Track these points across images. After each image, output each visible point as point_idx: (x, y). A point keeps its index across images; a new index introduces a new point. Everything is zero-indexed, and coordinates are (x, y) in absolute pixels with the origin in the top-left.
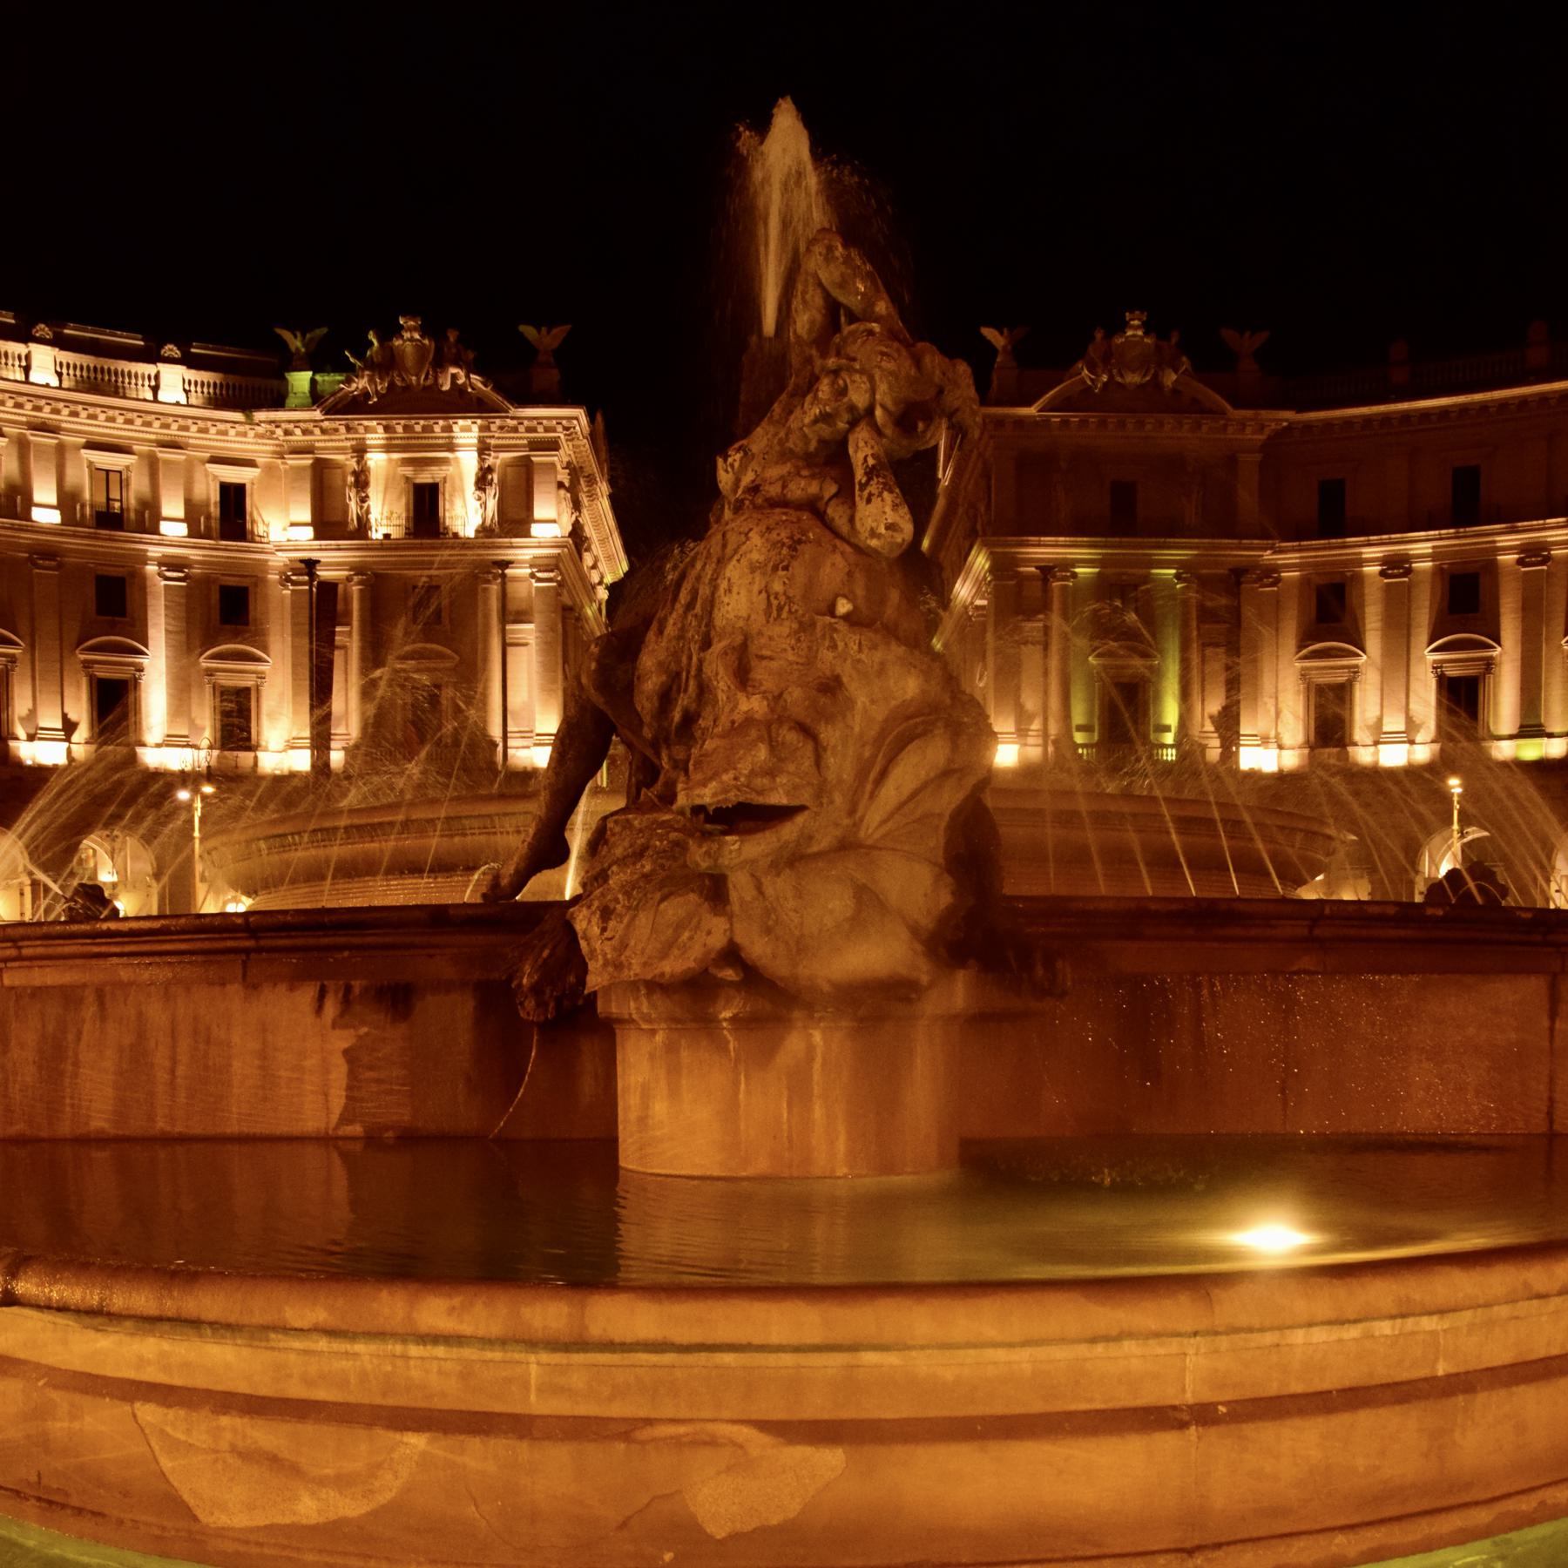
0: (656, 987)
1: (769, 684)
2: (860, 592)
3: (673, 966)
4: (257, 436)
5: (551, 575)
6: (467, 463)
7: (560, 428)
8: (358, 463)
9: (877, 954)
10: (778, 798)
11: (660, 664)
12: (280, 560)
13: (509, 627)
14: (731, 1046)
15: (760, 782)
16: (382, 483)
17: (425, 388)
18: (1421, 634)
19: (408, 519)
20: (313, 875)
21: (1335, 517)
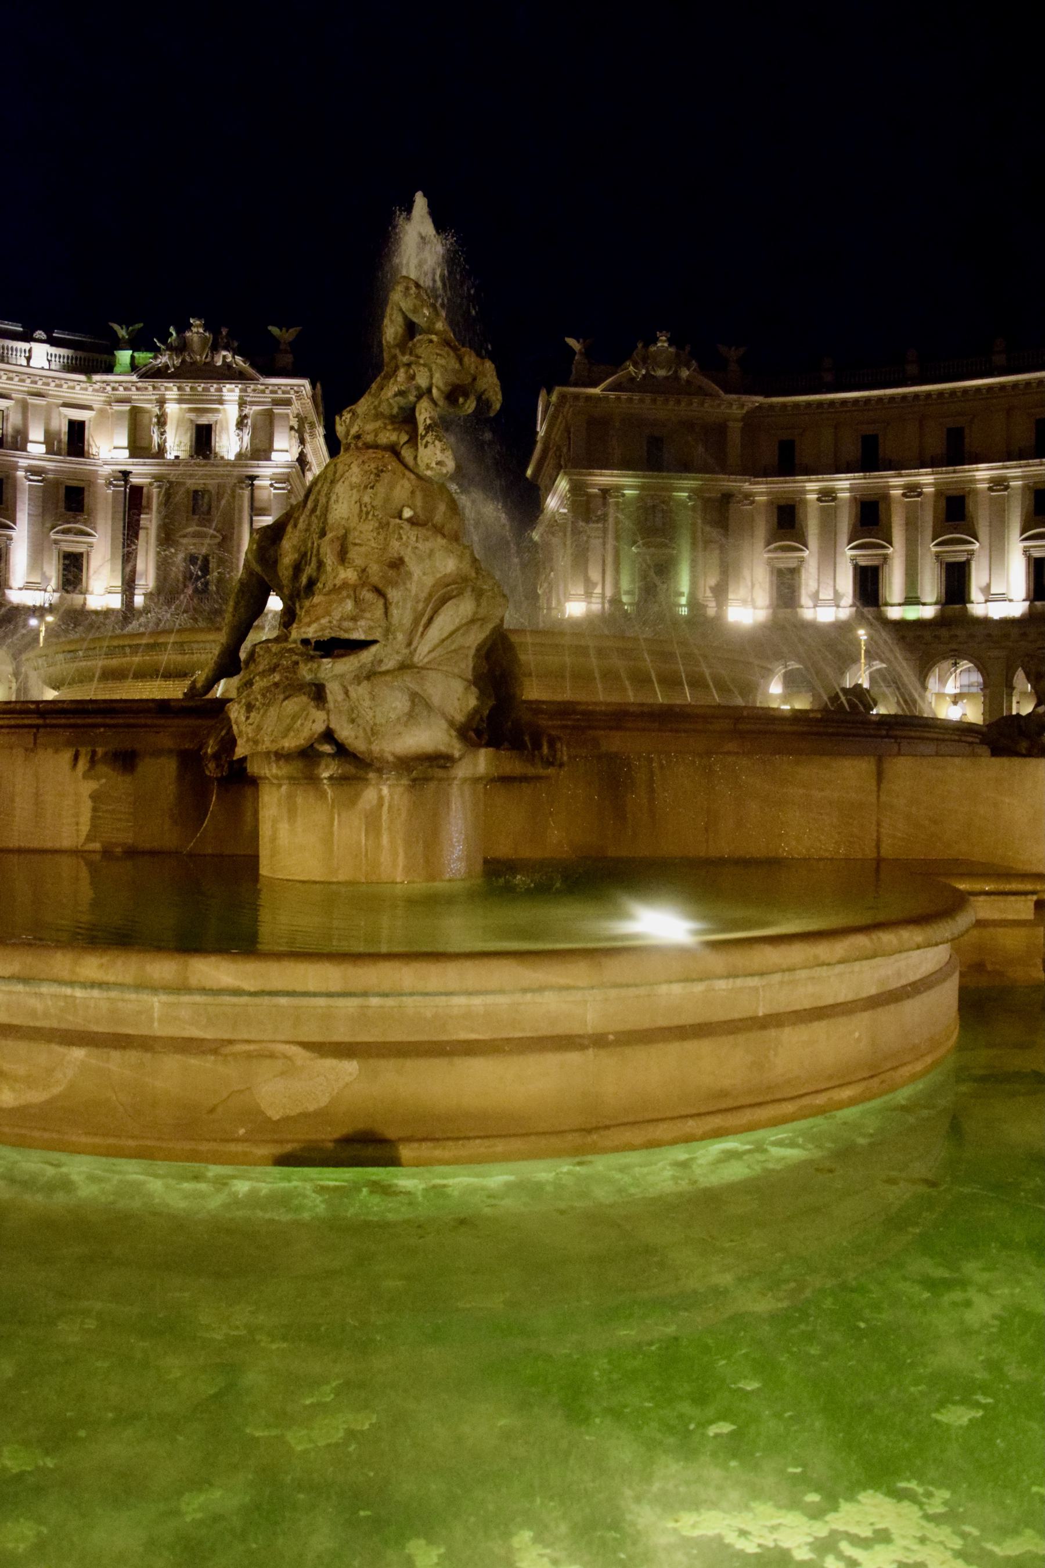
0: (280, 756)
1: (359, 562)
2: (419, 502)
3: (290, 743)
4: (94, 390)
5: (284, 485)
6: (230, 412)
7: (292, 392)
8: (160, 409)
9: (428, 737)
10: (358, 635)
11: (294, 546)
12: (106, 470)
13: (255, 518)
14: (329, 796)
15: (346, 624)
16: (175, 422)
17: (205, 363)
19: (191, 447)
20: (111, 675)
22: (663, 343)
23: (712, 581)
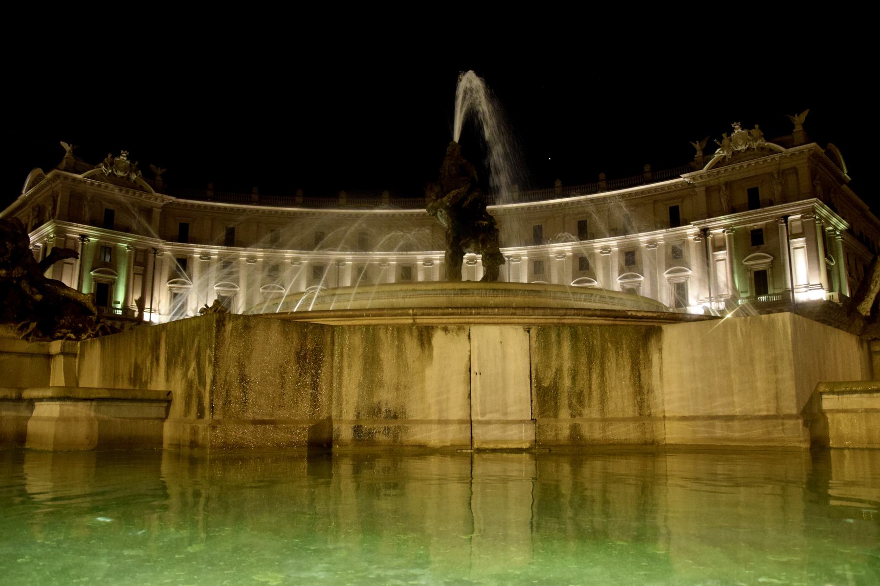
21: (184, 236)
23: (137, 296)
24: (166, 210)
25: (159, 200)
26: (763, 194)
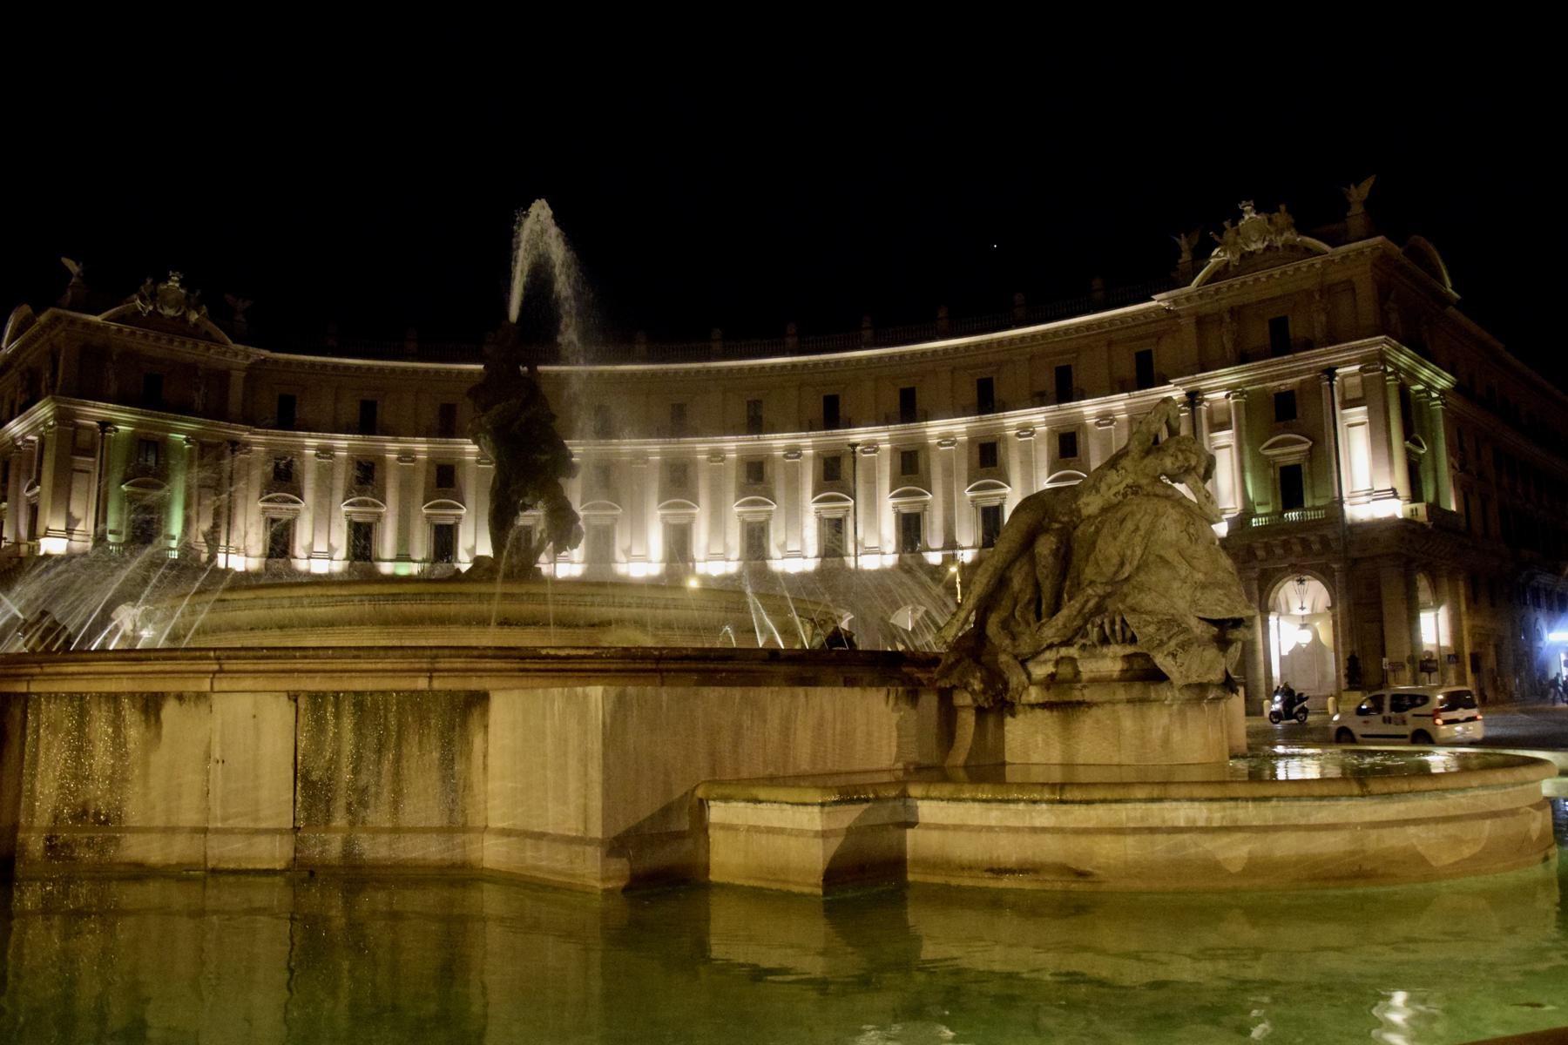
18: (339, 494)
21: (288, 418)
22: (174, 283)
23: (205, 526)
24: (255, 373)
25: (240, 356)
26: (1296, 329)
